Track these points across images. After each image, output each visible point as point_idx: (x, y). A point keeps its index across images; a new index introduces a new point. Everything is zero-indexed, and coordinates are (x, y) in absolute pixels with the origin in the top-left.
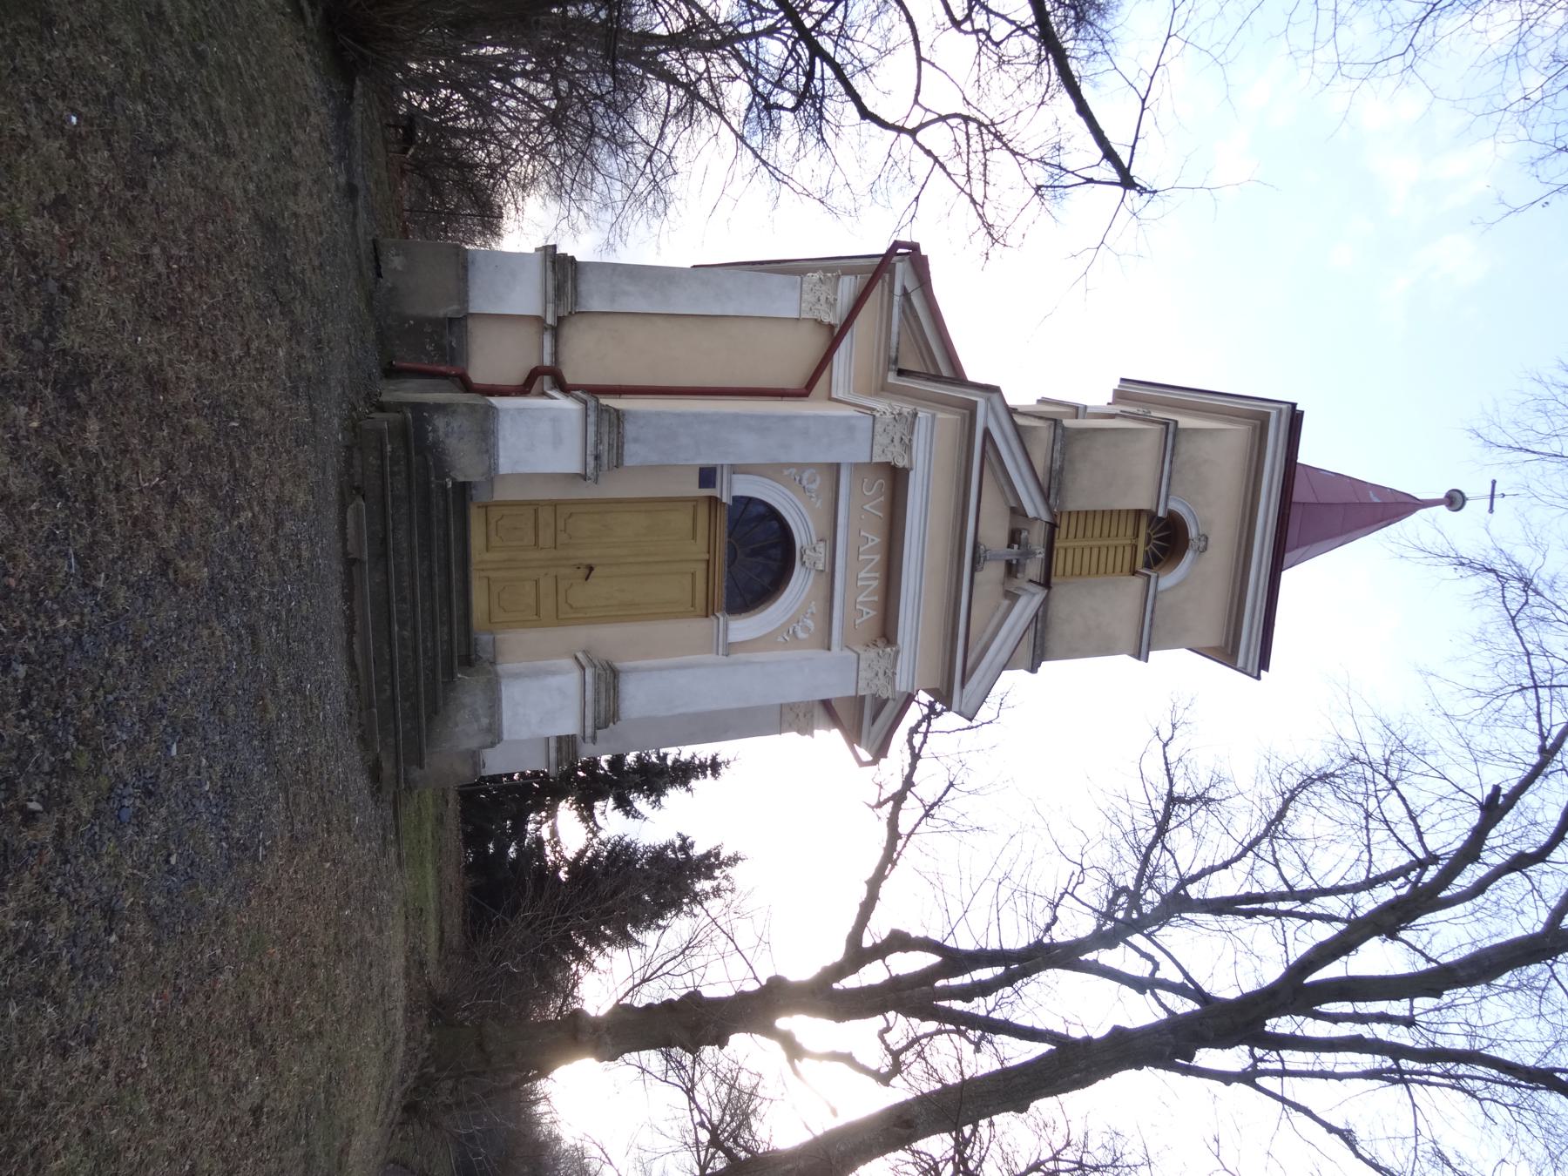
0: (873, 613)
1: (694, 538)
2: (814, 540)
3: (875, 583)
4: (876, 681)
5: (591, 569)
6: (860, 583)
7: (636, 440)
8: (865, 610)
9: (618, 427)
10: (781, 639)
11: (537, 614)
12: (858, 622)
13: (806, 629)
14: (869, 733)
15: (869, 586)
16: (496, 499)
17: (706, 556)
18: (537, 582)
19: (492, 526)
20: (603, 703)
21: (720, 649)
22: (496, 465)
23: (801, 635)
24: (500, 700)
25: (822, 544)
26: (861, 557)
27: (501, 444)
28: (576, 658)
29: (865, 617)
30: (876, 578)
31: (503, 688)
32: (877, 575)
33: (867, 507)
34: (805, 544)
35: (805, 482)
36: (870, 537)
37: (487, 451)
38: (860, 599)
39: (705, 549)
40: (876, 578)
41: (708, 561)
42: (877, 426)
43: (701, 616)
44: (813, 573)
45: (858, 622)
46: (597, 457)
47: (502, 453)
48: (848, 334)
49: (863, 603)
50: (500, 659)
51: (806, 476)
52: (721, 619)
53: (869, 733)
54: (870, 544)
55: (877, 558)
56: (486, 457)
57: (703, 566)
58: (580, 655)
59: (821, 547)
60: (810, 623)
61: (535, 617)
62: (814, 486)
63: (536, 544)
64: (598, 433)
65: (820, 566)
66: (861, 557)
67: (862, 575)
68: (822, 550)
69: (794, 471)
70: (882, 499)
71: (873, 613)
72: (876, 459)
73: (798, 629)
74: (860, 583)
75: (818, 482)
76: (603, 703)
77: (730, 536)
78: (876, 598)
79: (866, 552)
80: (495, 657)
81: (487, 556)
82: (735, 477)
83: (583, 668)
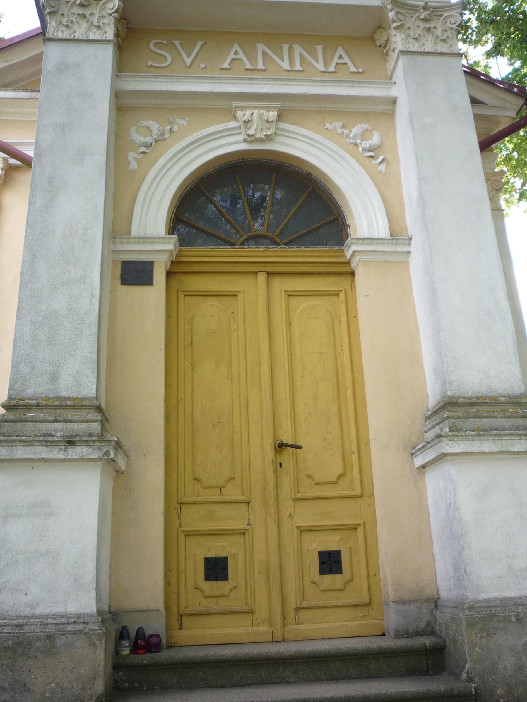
0: (340, 51)
1: (234, 295)
2: (233, 124)
3: (298, 49)
4: (439, 32)
5: (281, 446)
6: (298, 67)
7: (54, 378)
8: (336, 60)
9: (28, 407)
10: (383, 167)
11: (355, 528)
12: (353, 69)
13: (365, 135)
14: (495, 107)
15: (302, 58)
16: (159, 603)
17: (262, 278)
18: (302, 530)
19: (212, 605)
20: (500, 422)
21: (400, 249)
22: (77, 619)
23: (375, 140)
24: (504, 602)
25: (239, 114)
26: (261, 66)
27: (41, 610)
28: (424, 467)
29: (346, 60)
30: (291, 51)
31: (483, 596)
32: (286, 47)
33: (188, 61)
34: (241, 137)
35: (149, 140)
36: (231, 56)
37: (50, 637)
38: (321, 67)
39: (251, 278)
40: (291, 51)
41: (269, 274)
42: (60, 36)
43: (353, 281)
44: (282, 125)
45: (353, 69)
46: (70, 442)
47: (60, 609)
48: (20, 148)
49: (326, 65)
50: (429, 592)
51: (139, 138)
52: (353, 248)
53: (495, 107)
54: (241, 55)
55: (261, 47)
56: (60, 642)
57: (276, 281)
58: (419, 461)
59: (243, 115)
60: (356, 129)
61: (360, 529)
62: (155, 127)
63: (242, 533)
64: (28, 443)
65: (273, 115)
66: (261, 66)
67: (286, 65)
68: (248, 113)
69: (131, 156)
70: (177, 43)
71: (340, 51)
72: (110, 35)
73: (366, 144)
74: (298, 67)
75: (149, 123)
76: (500, 422)
77: (233, 244)
78: (319, 48)
79: (253, 59)
80: (427, 600)
81: (262, 612)
82: (134, 233)
83: (442, 457)
